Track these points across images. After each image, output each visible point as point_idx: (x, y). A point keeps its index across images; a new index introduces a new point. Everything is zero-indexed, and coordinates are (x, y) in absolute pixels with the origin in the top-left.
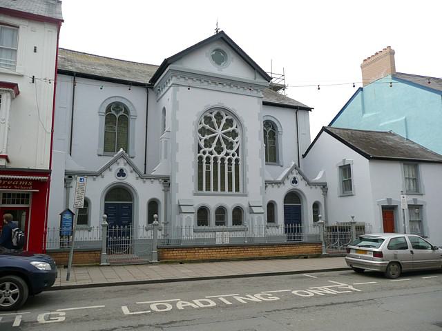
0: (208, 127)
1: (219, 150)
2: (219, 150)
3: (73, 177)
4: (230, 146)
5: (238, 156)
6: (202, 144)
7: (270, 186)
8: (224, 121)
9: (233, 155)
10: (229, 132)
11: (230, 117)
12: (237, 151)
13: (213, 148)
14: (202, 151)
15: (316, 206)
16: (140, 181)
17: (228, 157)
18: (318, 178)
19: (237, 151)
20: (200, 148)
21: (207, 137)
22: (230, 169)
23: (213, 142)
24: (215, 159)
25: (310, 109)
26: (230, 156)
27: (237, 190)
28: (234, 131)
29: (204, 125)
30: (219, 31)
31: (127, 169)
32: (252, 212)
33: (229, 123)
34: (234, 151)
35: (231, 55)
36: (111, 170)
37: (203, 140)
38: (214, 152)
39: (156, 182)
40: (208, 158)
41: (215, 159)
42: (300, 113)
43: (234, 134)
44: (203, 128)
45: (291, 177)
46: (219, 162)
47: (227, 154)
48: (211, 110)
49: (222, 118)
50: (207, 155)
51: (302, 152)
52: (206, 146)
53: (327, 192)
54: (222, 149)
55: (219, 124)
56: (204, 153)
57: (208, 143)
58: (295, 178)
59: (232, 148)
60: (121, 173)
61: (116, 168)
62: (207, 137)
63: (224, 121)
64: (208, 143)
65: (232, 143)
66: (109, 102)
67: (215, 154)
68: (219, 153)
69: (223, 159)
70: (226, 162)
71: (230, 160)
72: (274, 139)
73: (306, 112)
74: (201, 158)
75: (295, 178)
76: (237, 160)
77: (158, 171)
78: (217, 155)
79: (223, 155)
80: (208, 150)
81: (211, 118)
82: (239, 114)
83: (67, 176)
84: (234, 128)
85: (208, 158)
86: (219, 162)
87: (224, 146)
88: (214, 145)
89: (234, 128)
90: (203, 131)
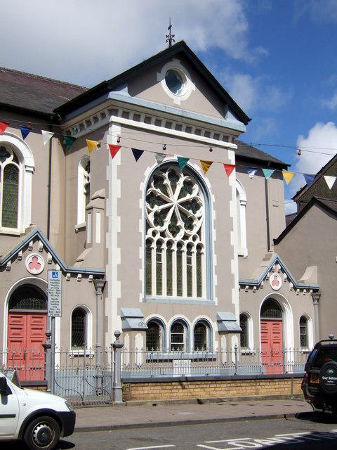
1: (174, 229)
2: (174, 229)
4: (189, 224)
6: (151, 218)
9: (194, 239)
12: (199, 232)
14: (150, 231)
17: (186, 242)
19: (199, 232)
21: (157, 208)
26: (190, 240)
28: (194, 200)
29: (154, 189)
30: (177, 40)
37: (152, 214)
38: (168, 232)
41: (170, 243)
44: (153, 194)
47: (186, 237)
49: (178, 178)
50: (158, 237)
51: (275, 235)
54: (178, 229)
55: (174, 187)
56: (154, 234)
57: (159, 217)
62: (157, 208)
64: (159, 217)
65: (191, 220)
67: (169, 236)
68: (174, 234)
78: (172, 238)
80: (158, 228)
84: (194, 194)
87: (180, 223)
89: (194, 194)
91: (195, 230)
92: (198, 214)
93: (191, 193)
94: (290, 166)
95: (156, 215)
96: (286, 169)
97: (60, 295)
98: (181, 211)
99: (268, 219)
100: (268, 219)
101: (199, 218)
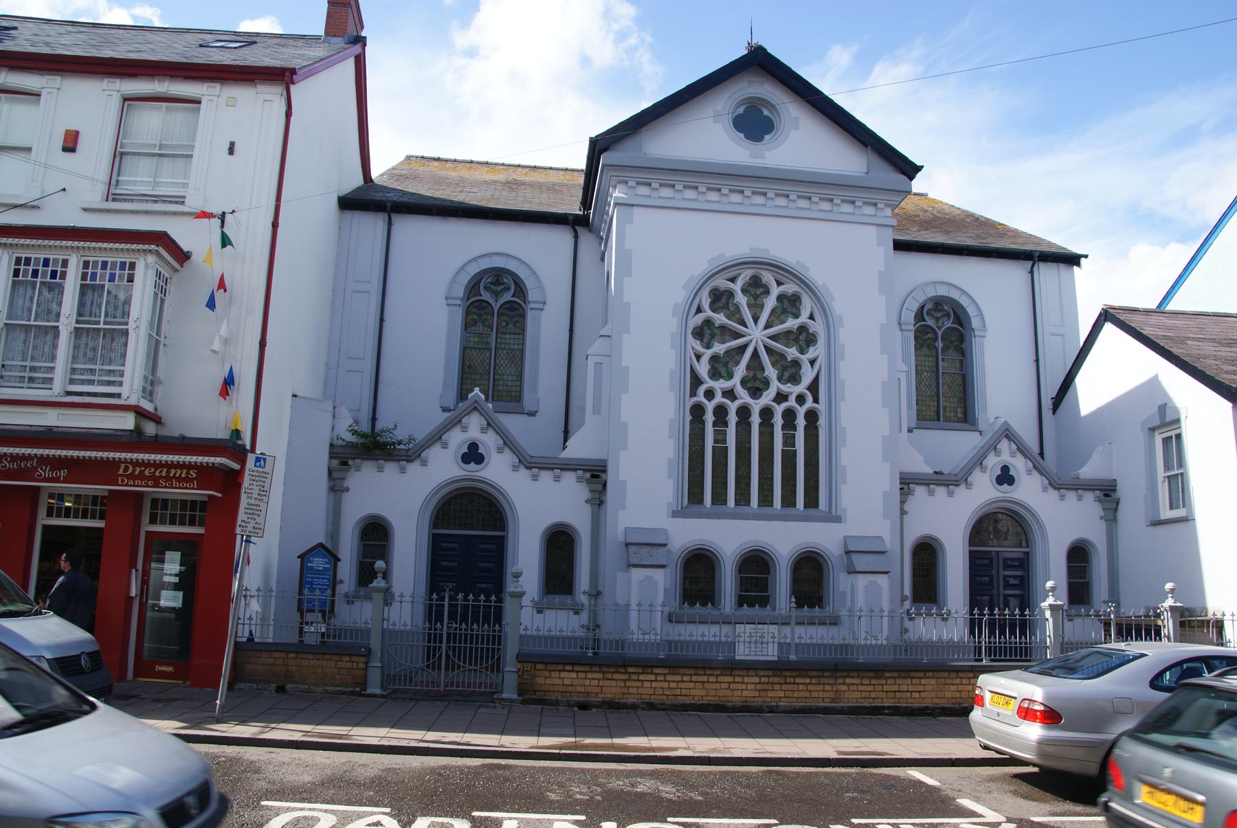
0: (720, 318)
2: (756, 386)
3: (350, 462)
4: (791, 372)
5: (816, 400)
6: (703, 369)
7: (920, 491)
8: (770, 303)
10: (788, 333)
11: (790, 288)
12: (814, 387)
13: (736, 381)
14: (701, 390)
15: (1079, 555)
16: (524, 473)
17: (784, 405)
18: (1090, 470)
19: (814, 387)
20: (696, 381)
21: (719, 348)
22: (789, 440)
23: (738, 363)
24: (744, 412)
25: (1073, 260)
27: (812, 500)
28: (803, 328)
29: (710, 313)
31: (489, 441)
32: (852, 571)
33: (790, 304)
34: (801, 388)
35: (791, 111)
36: (445, 446)
37: (705, 359)
38: (740, 391)
39: (569, 478)
40: (721, 412)
41: (744, 412)
42: (1046, 273)
43: (804, 338)
44: (708, 322)
45: (993, 463)
46: (755, 420)
47: (781, 397)
48: (731, 269)
50: (718, 399)
51: (1050, 391)
52: (715, 374)
53: (1116, 510)
54: (767, 383)
55: (756, 308)
56: (710, 394)
57: (720, 367)
58: (1005, 469)
59: (795, 379)
60: (473, 455)
61: (457, 439)
62: (719, 348)
63: (770, 303)
64: (720, 367)
65: (796, 364)
66: (474, 270)
67: (744, 397)
68: (756, 393)
69: (767, 413)
70: (778, 421)
71: (789, 415)
72: (962, 352)
73: (1062, 266)
74: (698, 411)
75: (1005, 469)
76: (812, 416)
77: (580, 447)
79: (767, 398)
80: (719, 385)
81: (730, 294)
82: (816, 276)
83: (335, 462)
84: (804, 318)
85: (721, 412)
86: (755, 420)
87: (771, 372)
88: (740, 371)
89: (804, 318)
90: (705, 332)
92: (811, 353)
93: (797, 316)
94: (1086, 256)
95: (714, 359)
96: (1078, 264)
97: (265, 499)
98: (769, 350)
101: (812, 362)
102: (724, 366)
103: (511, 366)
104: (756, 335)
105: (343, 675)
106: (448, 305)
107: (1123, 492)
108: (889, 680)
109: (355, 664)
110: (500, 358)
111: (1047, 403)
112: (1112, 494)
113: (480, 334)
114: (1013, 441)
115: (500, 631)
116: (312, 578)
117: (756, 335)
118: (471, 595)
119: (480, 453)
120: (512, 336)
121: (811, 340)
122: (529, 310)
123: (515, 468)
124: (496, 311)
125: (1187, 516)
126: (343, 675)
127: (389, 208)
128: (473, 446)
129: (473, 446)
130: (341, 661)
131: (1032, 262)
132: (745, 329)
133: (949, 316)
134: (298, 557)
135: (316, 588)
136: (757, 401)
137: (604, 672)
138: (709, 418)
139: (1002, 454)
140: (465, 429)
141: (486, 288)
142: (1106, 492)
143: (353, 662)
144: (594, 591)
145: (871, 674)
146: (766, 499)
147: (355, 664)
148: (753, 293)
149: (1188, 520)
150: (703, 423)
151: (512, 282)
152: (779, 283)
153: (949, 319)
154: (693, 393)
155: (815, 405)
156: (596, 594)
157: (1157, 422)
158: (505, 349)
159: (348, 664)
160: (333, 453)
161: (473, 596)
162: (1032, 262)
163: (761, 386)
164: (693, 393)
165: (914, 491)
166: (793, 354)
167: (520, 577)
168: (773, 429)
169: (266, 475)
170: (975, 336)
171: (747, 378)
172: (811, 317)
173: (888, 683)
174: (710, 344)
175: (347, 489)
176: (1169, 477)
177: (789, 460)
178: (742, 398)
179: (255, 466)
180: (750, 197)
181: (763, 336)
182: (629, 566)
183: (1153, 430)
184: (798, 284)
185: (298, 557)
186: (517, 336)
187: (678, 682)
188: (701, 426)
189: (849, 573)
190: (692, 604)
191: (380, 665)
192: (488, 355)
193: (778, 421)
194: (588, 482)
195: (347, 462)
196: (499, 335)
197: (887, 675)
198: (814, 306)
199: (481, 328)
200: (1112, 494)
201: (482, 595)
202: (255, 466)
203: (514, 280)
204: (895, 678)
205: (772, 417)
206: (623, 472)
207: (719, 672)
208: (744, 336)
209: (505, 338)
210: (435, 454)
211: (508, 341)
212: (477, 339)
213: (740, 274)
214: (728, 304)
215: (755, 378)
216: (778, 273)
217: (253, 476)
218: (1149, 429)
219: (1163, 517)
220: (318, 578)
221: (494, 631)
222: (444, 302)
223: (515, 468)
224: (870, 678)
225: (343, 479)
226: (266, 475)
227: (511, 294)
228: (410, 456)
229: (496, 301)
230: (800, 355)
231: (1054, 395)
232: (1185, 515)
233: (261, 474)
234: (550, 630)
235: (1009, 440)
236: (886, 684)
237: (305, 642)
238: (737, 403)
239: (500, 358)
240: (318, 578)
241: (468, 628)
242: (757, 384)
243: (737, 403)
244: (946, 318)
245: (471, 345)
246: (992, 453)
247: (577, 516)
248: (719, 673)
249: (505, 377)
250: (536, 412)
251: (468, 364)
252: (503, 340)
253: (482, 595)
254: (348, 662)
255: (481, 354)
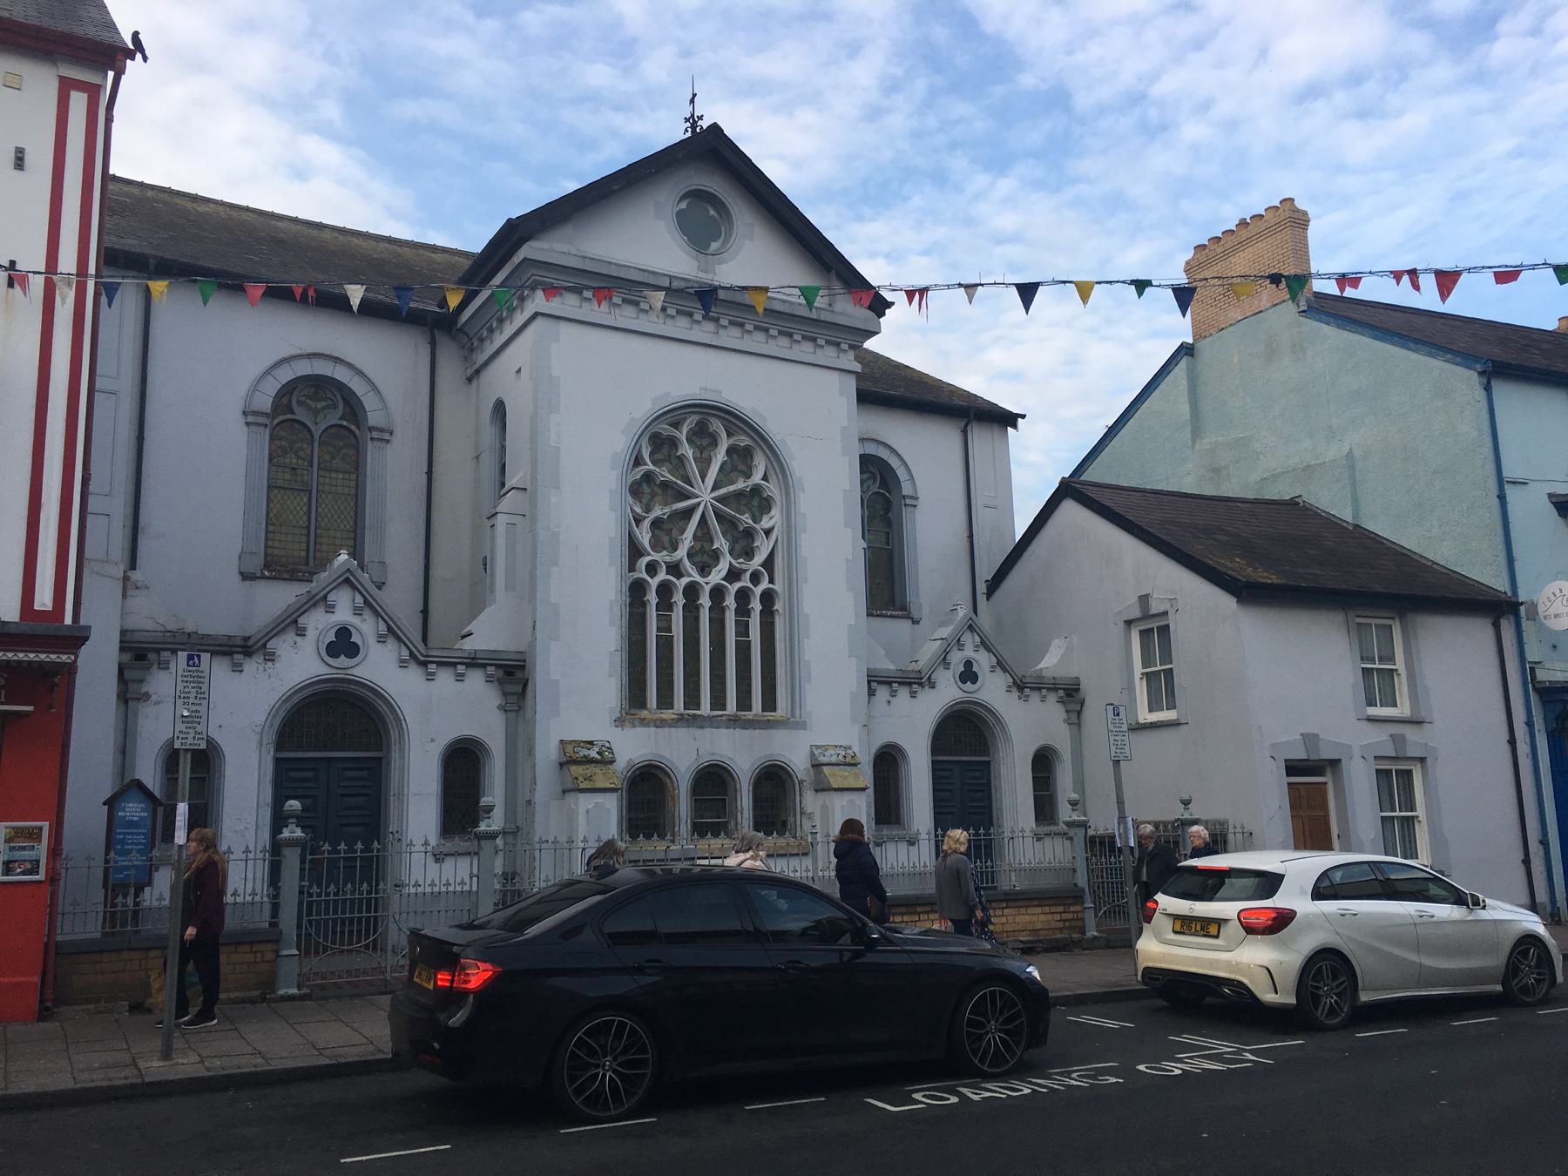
0: (664, 474)
1: (705, 558)
2: (705, 558)
3: (152, 656)
4: (744, 542)
5: (771, 581)
6: (644, 537)
7: (882, 693)
8: (720, 456)
9: (756, 578)
10: (739, 494)
11: (743, 441)
12: (769, 563)
13: (682, 553)
14: (644, 561)
15: (1043, 762)
16: (414, 674)
17: (737, 585)
18: (1051, 662)
19: (769, 563)
20: (635, 551)
22: (743, 629)
23: (683, 531)
24: (692, 591)
25: (1008, 419)
26: (745, 582)
27: (770, 703)
28: (756, 490)
29: (651, 467)
30: (705, 124)
31: (366, 629)
32: (822, 788)
33: (740, 459)
36: (301, 632)
37: (646, 524)
39: (476, 679)
40: (665, 590)
42: (980, 438)
43: (758, 501)
44: (648, 477)
45: (957, 658)
46: (705, 601)
47: (733, 575)
48: (675, 415)
49: (714, 443)
50: (662, 575)
51: (985, 572)
52: (657, 545)
53: (1079, 713)
54: (716, 556)
56: (652, 568)
57: (665, 532)
58: (968, 664)
59: (749, 554)
60: (343, 644)
61: (320, 625)
63: (720, 456)
65: (749, 534)
66: (286, 375)
68: (704, 570)
69: (718, 593)
70: (730, 602)
71: (743, 595)
72: (889, 523)
73: (996, 430)
74: (637, 590)
75: (968, 664)
76: (768, 598)
77: (487, 634)
78: (698, 578)
79: (717, 576)
80: (662, 557)
81: (673, 443)
82: (774, 428)
83: (127, 657)
84: (757, 478)
85: (665, 590)
86: (705, 601)
87: (721, 543)
88: (687, 540)
90: (642, 488)
91: (759, 558)
92: (766, 523)
93: (748, 475)
94: (1023, 416)
95: (656, 524)
96: (1015, 426)
98: (720, 516)
99: (430, 473)
100: (430, 473)
101: (768, 532)
102: (667, 535)
103: (332, 516)
104: (705, 494)
105: (241, 973)
106: (248, 424)
107: (1089, 689)
108: (921, 916)
109: (259, 955)
110: (324, 506)
111: (981, 588)
112: (1075, 694)
113: (293, 468)
114: (977, 633)
115: (992, 867)
116: (124, 834)
117: (705, 494)
118: (343, 844)
119: (974, 672)
120: (341, 476)
121: (765, 505)
122: (370, 444)
123: (403, 664)
124: (317, 437)
125: (1178, 719)
126: (241, 973)
127: (152, 267)
128: (343, 632)
129: (343, 632)
130: (236, 952)
131: (966, 420)
132: (691, 488)
133: (875, 479)
134: (104, 804)
135: (130, 851)
136: (706, 580)
137: (1065, 905)
138: (652, 598)
139: (965, 648)
140: (330, 609)
141: (299, 403)
142: (1069, 692)
143: (255, 952)
144: (514, 827)
145: (903, 910)
146: (665, 700)
147: (259, 955)
148: (699, 443)
149: (1180, 724)
150: (644, 605)
151: (338, 396)
152: (729, 435)
153: (875, 481)
154: (632, 568)
155: (771, 586)
156: (512, 832)
157: (1136, 613)
158: (330, 493)
159: (249, 955)
160: (125, 642)
161: (345, 845)
162: (966, 420)
163: (710, 561)
164: (632, 568)
165: (875, 690)
166: (746, 523)
167: (1190, 803)
168: (645, 610)
169: (202, 680)
170: (905, 505)
171: (694, 551)
172: (765, 478)
173: (921, 918)
174: (650, 505)
175: (147, 696)
176: (1146, 674)
177: (665, 646)
178: (690, 576)
179: (188, 665)
180: (674, 317)
181: (713, 499)
182: (564, 792)
183: (1129, 623)
184: (751, 436)
185: (104, 804)
186: (347, 476)
187: (1061, 913)
188: (641, 610)
189: (817, 791)
190: (702, 835)
191: (297, 953)
192: (305, 499)
193: (730, 602)
194: (500, 682)
195: (146, 655)
196: (322, 473)
197: (919, 909)
198: (769, 466)
199: (295, 461)
200: (1075, 694)
201: (359, 842)
202: (188, 665)
203: (343, 398)
204: (928, 912)
205: (723, 600)
206: (549, 670)
207: (1005, 905)
208: (689, 498)
209: (331, 478)
210: (283, 645)
211: (334, 482)
212: (287, 476)
213: (685, 419)
214: (669, 456)
215: (702, 551)
216: (735, 424)
217: (187, 682)
218: (1125, 622)
219: (1141, 721)
220: (133, 834)
221: (987, 868)
222: (242, 420)
223: (403, 664)
224: (902, 914)
225: (142, 681)
226: (202, 680)
227: (340, 414)
228: (250, 647)
229: (316, 424)
230: (754, 525)
231: (990, 578)
232: (1175, 718)
233: (196, 679)
234: (433, 884)
235: (972, 631)
236: (919, 920)
237: (999, 889)
238: (685, 581)
239: (324, 506)
240: (133, 834)
241: (371, 889)
242: (706, 558)
243: (685, 581)
244: (871, 482)
245: (280, 483)
246: (955, 649)
247: (1058, 735)
248: (1005, 905)
249: (332, 533)
250: (384, 583)
251: (275, 511)
252: (327, 481)
253: (359, 842)
254: (247, 953)
255: (295, 498)
